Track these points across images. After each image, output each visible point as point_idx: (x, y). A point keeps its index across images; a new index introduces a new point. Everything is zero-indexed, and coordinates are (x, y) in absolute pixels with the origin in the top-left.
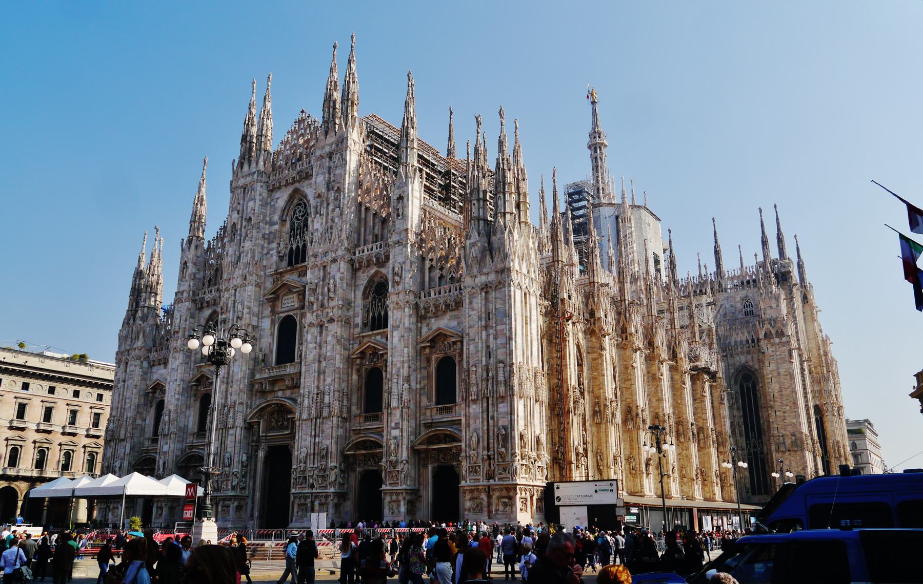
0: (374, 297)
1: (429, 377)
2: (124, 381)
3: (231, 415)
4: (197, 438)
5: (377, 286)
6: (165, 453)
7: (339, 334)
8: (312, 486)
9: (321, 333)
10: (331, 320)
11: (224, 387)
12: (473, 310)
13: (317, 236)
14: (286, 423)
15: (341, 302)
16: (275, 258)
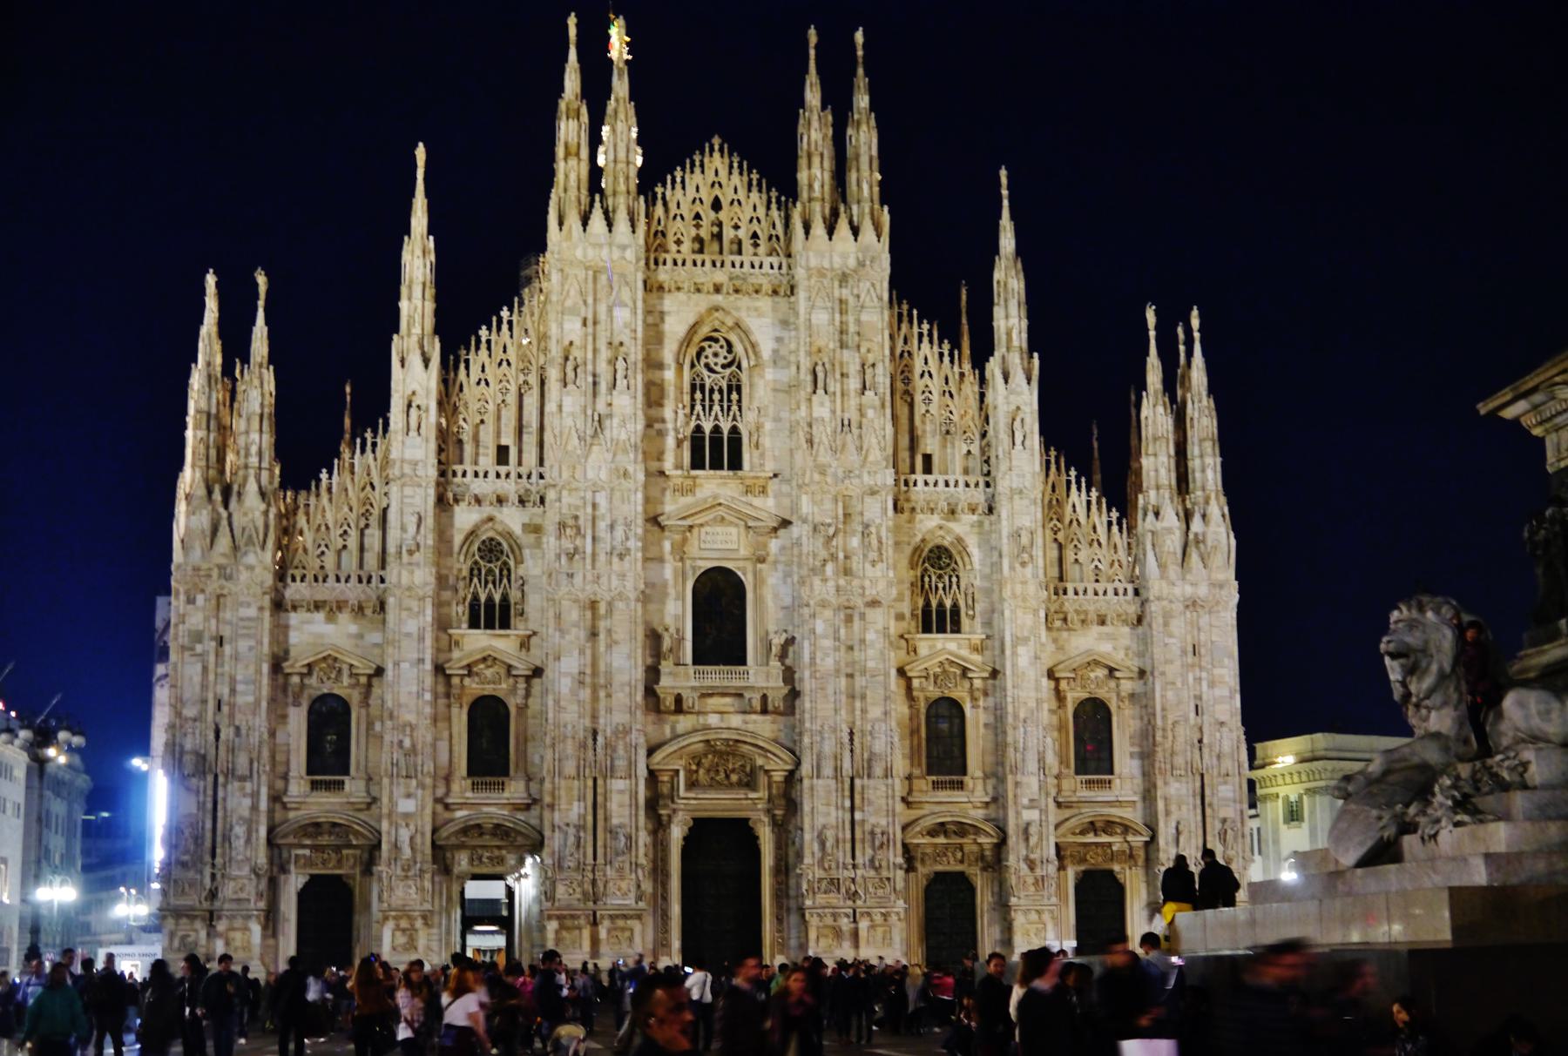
0: (926, 570)
1: (1061, 728)
2: (220, 641)
3: (621, 751)
4: (474, 787)
5: (931, 551)
6: (407, 816)
7: (892, 631)
8: (854, 896)
9: (849, 619)
10: (874, 603)
11: (586, 694)
12: (1171, 636)
13: (822, 434)
14: (734, 778)
15: (891, 574)
16: (670, 442)
